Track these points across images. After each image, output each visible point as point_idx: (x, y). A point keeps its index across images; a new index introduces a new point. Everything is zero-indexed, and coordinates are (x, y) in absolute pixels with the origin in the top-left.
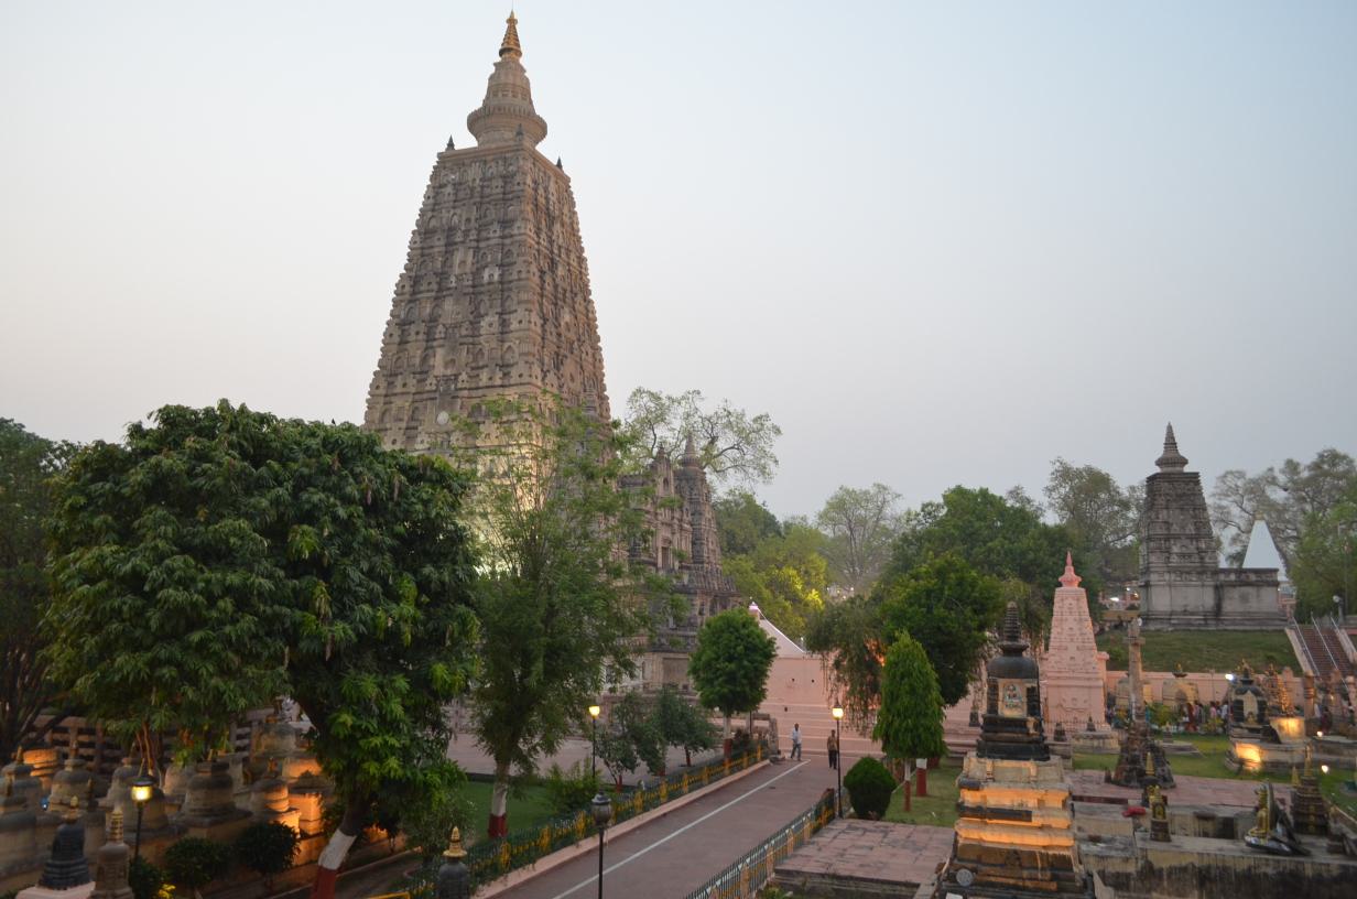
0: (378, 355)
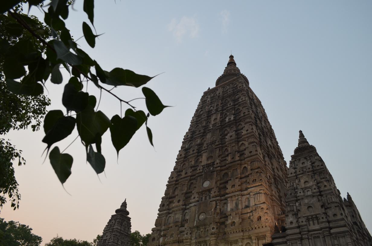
0: (174, 164)
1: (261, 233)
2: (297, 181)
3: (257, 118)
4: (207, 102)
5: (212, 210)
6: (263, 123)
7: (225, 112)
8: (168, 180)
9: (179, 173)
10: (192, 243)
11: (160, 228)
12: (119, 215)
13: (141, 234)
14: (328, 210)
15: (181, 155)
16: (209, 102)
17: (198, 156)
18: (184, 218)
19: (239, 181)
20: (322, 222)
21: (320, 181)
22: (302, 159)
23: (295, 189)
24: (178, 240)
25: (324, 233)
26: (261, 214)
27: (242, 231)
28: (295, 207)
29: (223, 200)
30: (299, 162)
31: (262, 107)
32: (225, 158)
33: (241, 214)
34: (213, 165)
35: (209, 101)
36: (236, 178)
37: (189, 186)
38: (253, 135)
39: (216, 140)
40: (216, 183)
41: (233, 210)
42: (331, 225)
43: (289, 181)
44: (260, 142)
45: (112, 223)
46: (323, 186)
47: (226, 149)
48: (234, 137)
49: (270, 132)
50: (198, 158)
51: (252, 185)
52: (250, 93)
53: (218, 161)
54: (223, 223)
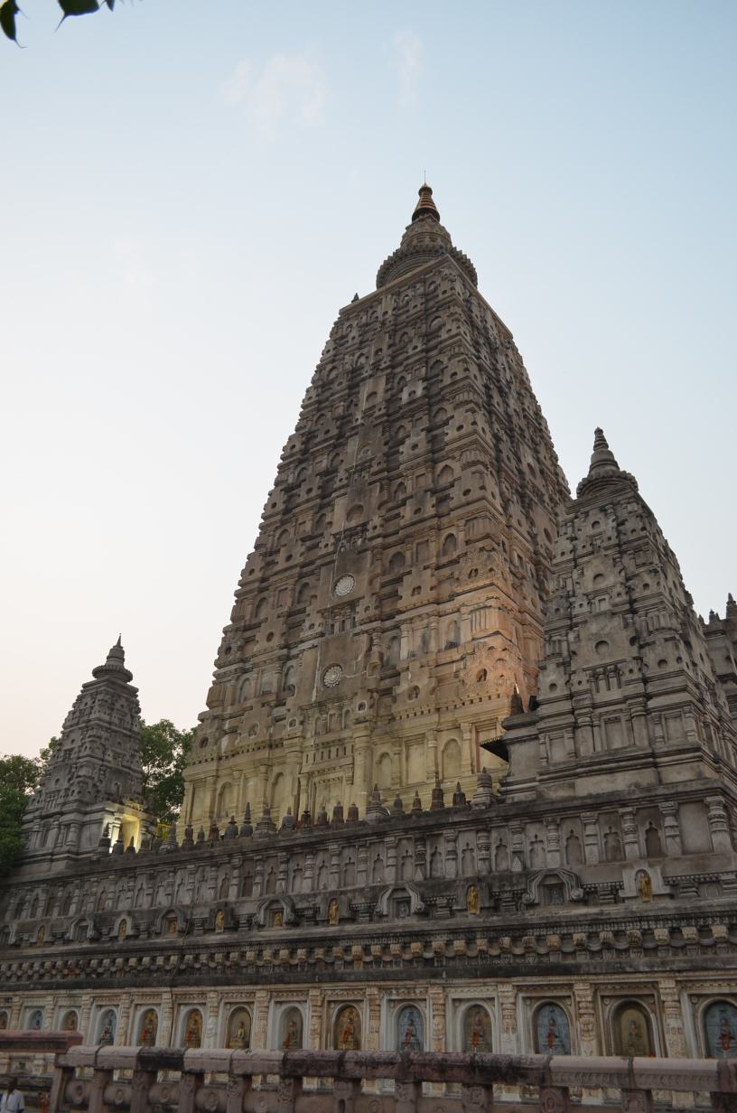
1: (486, 713)
2: (575, 575)
3: (492, 386)
4: (350, 341)
5: (359, 659)
6: (512, 402)
7: (401, 372)
8: (241, 578)
9: (269, 559)
10: (306, 747)
11: (220, 713)
12: (104, 681)
13: (176, 728)
14: (646, 649)
15: (274, 505)
16: (356, 340)
17: (321, 507)
18: (285, 683)
19: (433, 575)
20: (629, 682)
21: (633, 572)
22: (594, 512)
23: (568, 597)
24: (270, 740)
25: (632, 710)
26: (487, 663)
27: (438, 710)
28: (564, 645)
29: (388, 630)
30: (584, 521)
31: (515, 349)
32: (396, 512)
33: (436, 666)
34: (363, 531)
35: (354, 338)
36: (425, 568)
37: (297, 595)
38: (476, 442)
39: (372, 460)
40: (371, 582)
41: (414, 656)
42: (651, 689)
43: (556, 575)
44: (498, 459)
45: (86, 704)
46: (641, 586)
47: (402, 484)
48: (423, 447)
49: (535, 428)
50: (323, 512)
51: (467, 584)
52: (475, 310)
53: (376, 521)
54: (387, 692)
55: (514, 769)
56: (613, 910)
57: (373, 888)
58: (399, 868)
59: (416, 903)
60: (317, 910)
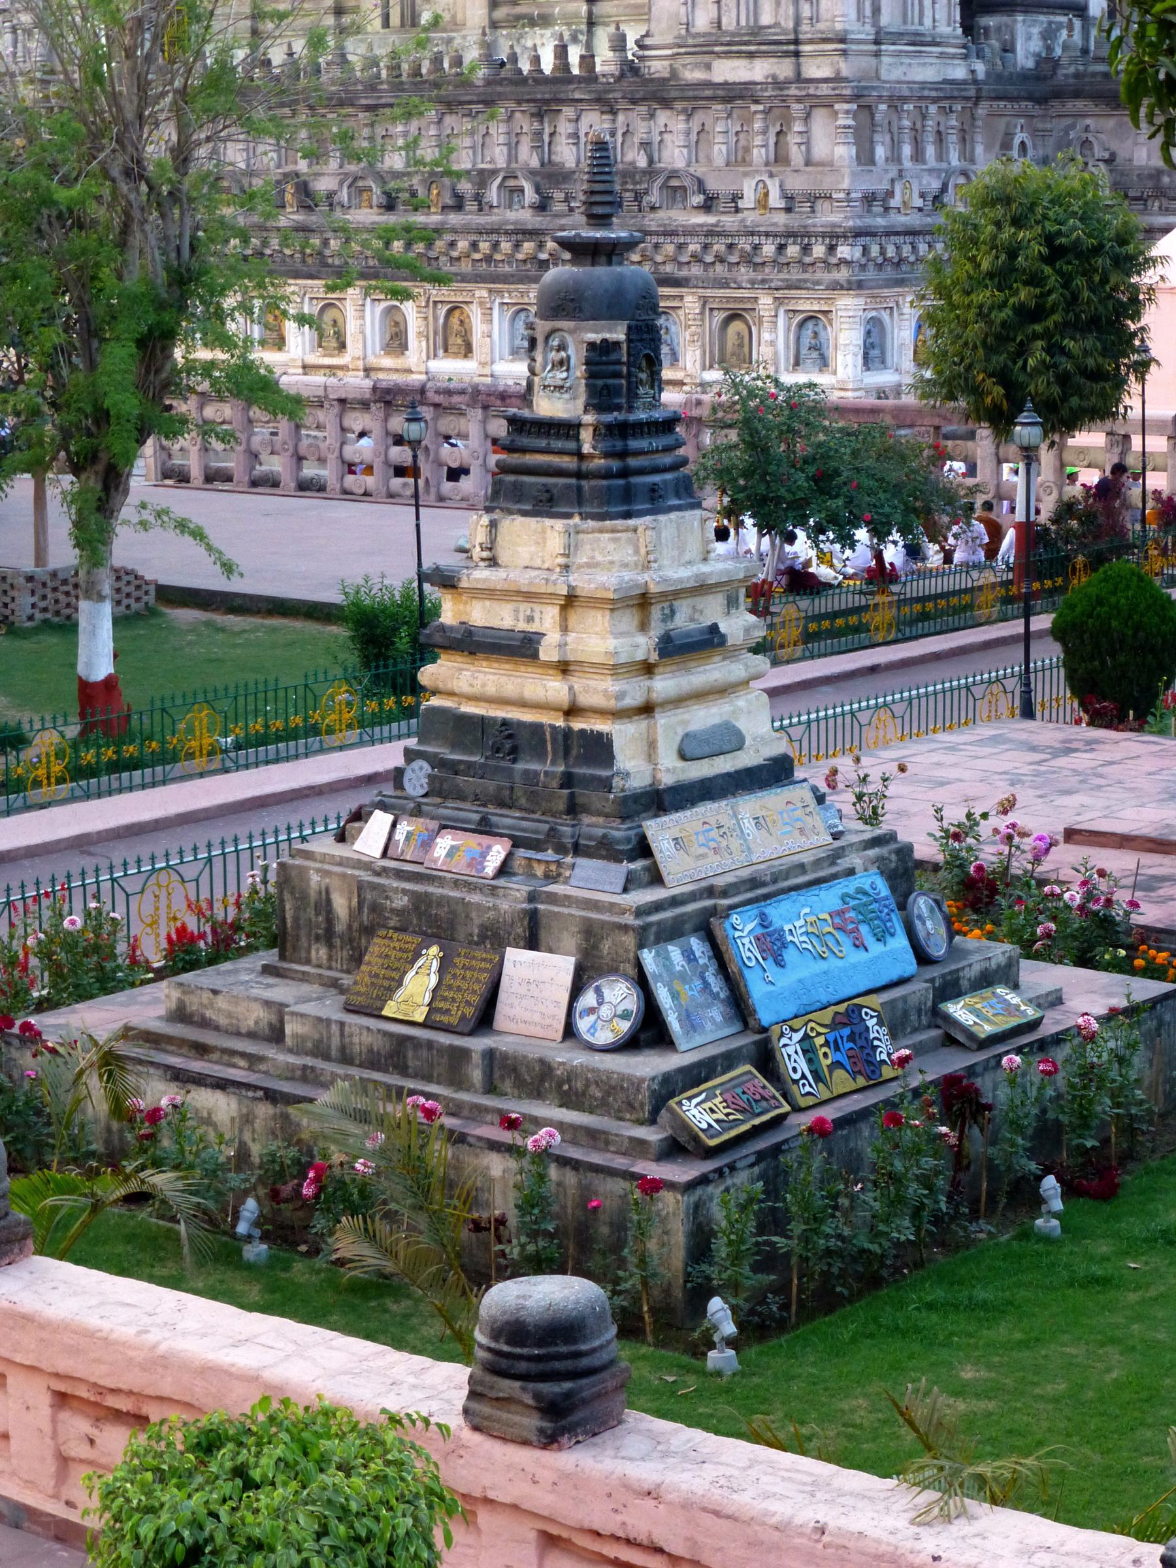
55: (654, 28)
56: (729, 221)
57: (482, 172)
58: (512, 148)
59: (530, 196)
60: (414, 194)
